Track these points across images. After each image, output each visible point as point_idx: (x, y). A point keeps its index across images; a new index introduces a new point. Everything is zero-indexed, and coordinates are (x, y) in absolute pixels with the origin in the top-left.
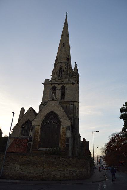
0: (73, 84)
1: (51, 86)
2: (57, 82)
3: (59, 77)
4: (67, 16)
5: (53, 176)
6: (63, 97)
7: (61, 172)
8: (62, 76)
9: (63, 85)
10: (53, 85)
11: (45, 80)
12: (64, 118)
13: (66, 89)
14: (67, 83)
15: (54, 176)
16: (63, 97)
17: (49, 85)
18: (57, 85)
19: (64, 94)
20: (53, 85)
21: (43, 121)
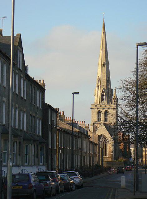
4: (104, 19)
6: (106, 119)
10: (99, 110)
11: (92, 104)
16: (106, 119)
18: (101, 110)
20: (99, 110)
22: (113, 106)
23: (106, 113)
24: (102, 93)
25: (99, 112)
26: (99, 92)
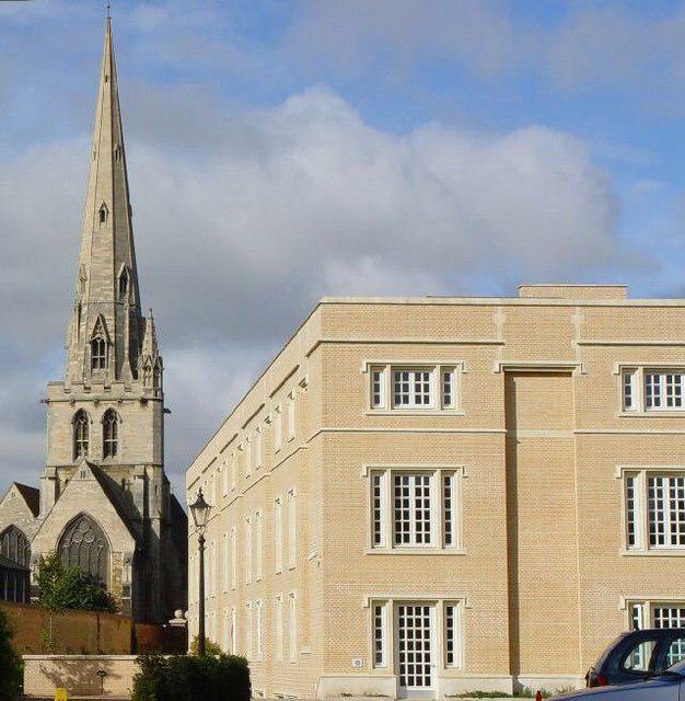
0: (144, 402)
1: (73, 411)
2: (91, 396)
6: (109, 449)
8: (102, 366)
9: (110, 406)
13: (121, 422)
16: (109, 449)
17: (63, 405)
18: (88, 407)
20: (78, 406)
21: (61, 540)
22: (140, 388)
23: (110, 419)
24: (95, 333)
25: (80, 417)
26: (83, 329)
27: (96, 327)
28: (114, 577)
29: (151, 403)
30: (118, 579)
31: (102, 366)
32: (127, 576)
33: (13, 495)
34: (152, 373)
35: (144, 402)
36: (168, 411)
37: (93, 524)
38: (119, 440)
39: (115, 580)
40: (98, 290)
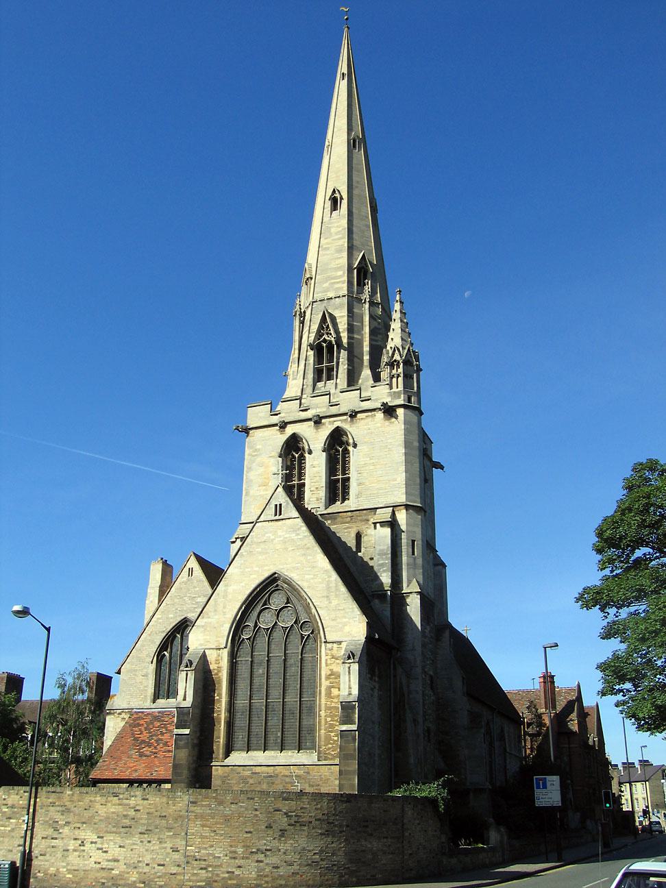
0: (389, 411)
1: (279, 439)
2: (308, 414)
3: (319, 380)
5: (227, 875)
6: (337, 489)
7: (261, 857)
9: (337, 423)
10: (290, 430)
12: (335, 602)
13: (355, 446)
14: (357, 413)
15: (233, 872)
18: (305, 430)
19: (345, 469)
20: (290, 430)
21: (239, 626)
27: (321, 327)
28: (329, 689)
29: (400, 412)
30: (335, 692)
31: (329, 378)
32: (349, 684)
33: (191, 571)
34: (401, 370)
35: (389, 411)
36: (439, 466)
37: (294, 594)
38: (353, 474)
39: (329, 694)
40: (326, 285)
